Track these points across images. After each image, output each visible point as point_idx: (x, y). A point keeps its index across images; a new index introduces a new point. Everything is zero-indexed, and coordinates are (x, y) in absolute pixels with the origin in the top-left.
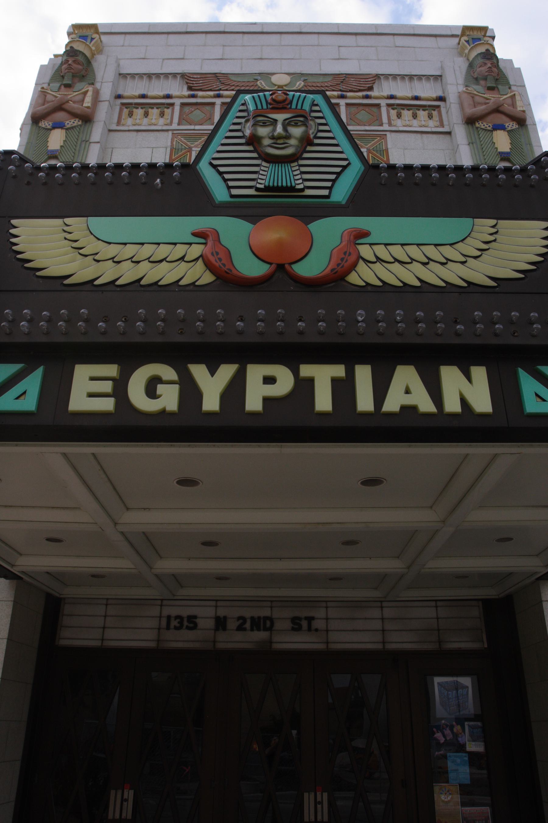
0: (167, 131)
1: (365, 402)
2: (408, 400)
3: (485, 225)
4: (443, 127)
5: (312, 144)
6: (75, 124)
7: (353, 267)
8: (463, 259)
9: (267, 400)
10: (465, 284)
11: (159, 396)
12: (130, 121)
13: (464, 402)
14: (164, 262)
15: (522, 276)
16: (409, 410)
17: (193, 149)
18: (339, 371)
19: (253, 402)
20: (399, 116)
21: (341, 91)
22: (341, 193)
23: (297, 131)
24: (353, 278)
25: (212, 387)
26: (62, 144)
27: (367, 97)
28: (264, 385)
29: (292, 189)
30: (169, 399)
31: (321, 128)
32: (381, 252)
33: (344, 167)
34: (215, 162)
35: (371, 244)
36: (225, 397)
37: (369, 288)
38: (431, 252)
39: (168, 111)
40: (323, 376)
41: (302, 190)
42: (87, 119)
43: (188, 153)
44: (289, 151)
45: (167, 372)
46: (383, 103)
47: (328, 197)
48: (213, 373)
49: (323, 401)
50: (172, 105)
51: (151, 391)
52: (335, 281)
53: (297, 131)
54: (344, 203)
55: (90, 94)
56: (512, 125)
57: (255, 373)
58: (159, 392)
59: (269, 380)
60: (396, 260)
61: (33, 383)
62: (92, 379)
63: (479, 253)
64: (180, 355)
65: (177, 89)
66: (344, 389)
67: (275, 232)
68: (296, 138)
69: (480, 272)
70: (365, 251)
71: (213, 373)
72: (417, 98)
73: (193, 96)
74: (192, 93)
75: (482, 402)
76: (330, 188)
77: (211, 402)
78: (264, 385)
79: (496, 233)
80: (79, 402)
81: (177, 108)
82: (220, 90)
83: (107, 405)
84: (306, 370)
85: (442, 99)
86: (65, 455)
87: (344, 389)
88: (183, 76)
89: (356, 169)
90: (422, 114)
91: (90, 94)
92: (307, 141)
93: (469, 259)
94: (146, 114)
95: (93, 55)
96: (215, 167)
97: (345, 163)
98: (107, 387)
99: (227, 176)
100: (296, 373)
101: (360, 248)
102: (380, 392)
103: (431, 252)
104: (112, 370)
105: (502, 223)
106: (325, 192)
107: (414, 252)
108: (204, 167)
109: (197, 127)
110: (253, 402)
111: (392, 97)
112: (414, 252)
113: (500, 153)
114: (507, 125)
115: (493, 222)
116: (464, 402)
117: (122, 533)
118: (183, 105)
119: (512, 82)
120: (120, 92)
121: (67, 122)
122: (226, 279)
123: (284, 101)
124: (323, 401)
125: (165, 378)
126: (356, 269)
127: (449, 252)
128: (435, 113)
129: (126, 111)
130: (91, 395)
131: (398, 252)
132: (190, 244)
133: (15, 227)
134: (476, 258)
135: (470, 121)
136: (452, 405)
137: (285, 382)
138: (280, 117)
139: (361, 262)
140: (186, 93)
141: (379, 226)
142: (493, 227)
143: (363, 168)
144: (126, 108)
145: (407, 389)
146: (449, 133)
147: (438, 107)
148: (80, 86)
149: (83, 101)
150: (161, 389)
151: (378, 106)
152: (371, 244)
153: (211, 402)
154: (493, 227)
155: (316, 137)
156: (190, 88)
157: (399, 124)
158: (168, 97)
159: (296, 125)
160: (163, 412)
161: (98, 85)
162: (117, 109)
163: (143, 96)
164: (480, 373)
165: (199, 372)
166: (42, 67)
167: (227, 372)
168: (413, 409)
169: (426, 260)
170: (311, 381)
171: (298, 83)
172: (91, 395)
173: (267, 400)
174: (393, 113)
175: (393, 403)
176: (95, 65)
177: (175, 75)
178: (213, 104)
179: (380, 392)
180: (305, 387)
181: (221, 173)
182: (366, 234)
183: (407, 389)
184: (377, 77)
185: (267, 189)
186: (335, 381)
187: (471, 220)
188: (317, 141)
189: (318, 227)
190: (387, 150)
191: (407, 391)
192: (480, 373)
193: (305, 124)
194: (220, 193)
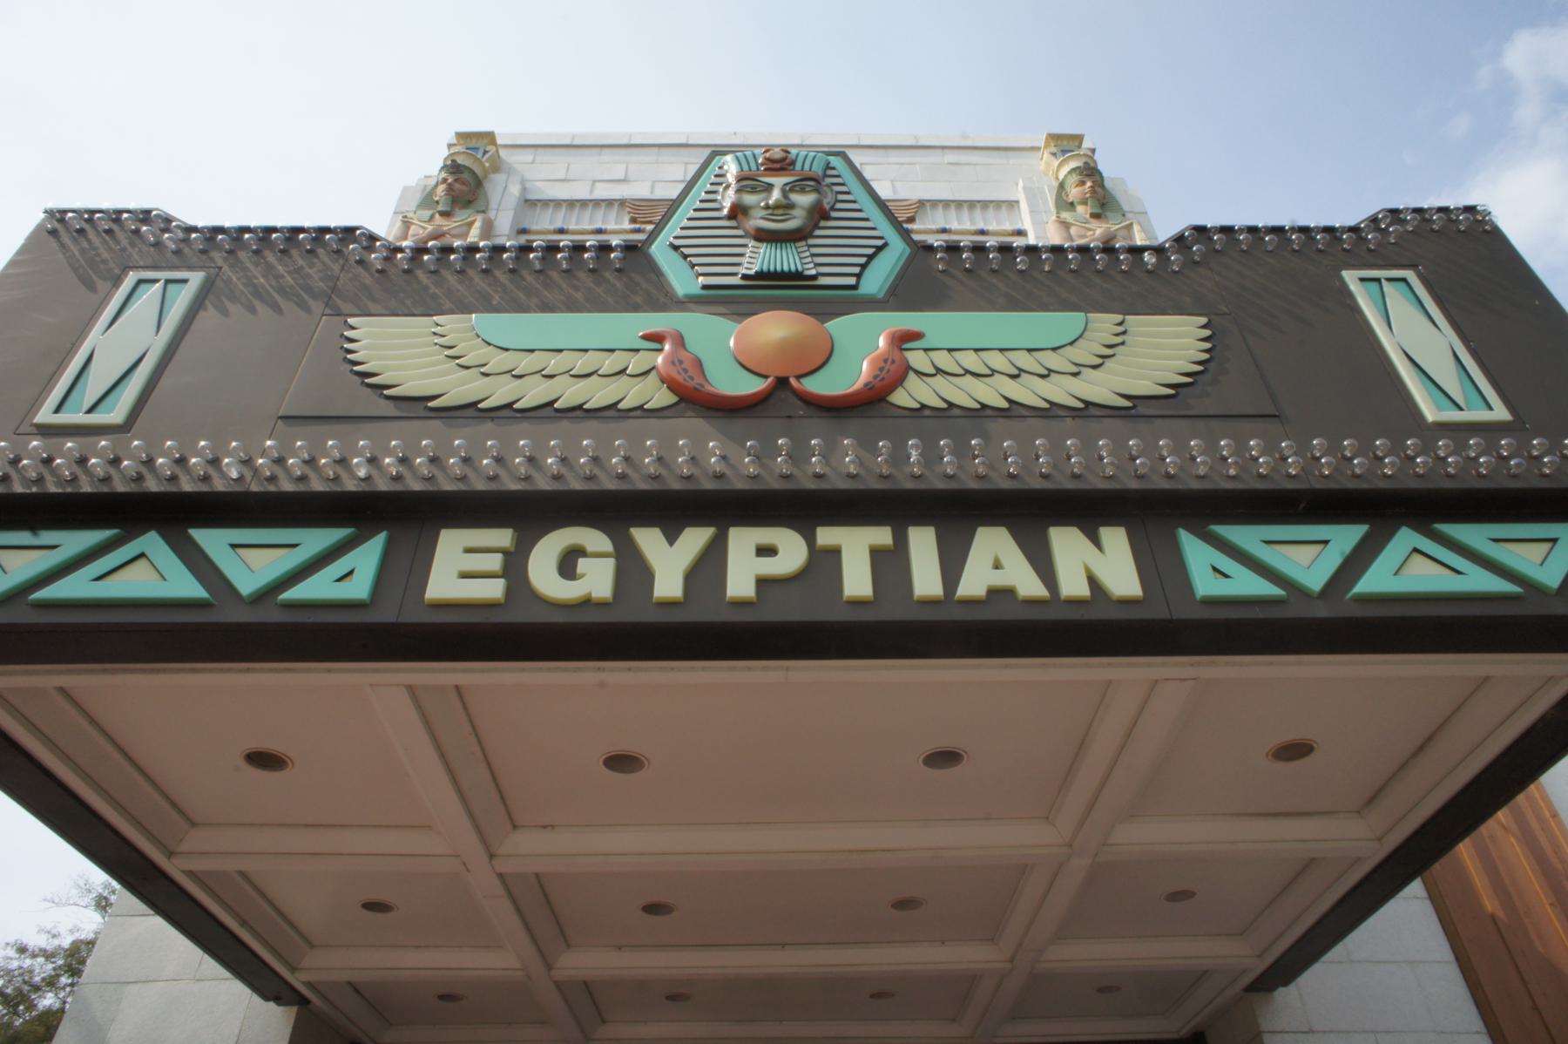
1: (926, 579)
2: (1000, 579)
3: (1104, 324)
5: (827, 217)
7: (898, 381)
8: (1075, 369)
9: (762, 583)
10: (1081, 405)
11: (582, 576)
13: (1093, 581)
14: (594, 377)
15: (1172, 392)
18: (882, 536)
22: (876, 280)
23: (804, 200)
24: (900, 398)
28: (755, 561)
29: (798, 275)
31: (841, 197)
32: (943, 360)
33: (879, 249)
34: (677, 242)
35: (926, 350)
36: (691, 576)
37: (927, 412)
38: (1024, 360)
40: (855, 547)
41: (814, 277)
44: (792, 224)
45: (595, 539)
47: (854, 287)
48: (671, 540)
49: (857, 581)
51: (568, 565)
52: (869, 404)
53: (804, 200)
54: (881, 295)
55: (477, 224)
57: (742, 541)
58: (579, 570)
59: (766, 551)
60: (967, 372)
61: (366, 559)
62: (469, 550)
63: (1099, 361)
64: (616, 510)
66: (890, 564)
67: (774, 328)
68: (802, 208)
69: (1101, 388)
70: (917, 359)
71: (671, 540)
73: (638, 231)
76: (859, 276)
77: (668, 583)
78: (755, 561)
79: (1124, 333)
83: (494, 590)
84: (827, 536)
86: (411, 689)
87: (890, 564)
88: (622, 203)
89: (898, 248)
91: (477, 224)
92: (819, 214)
93: (1084, 370)
95: (486, 173)
96: (676, 248)
97: (879, 243)
98: (494, 562)
99: (695, 260)
100: (810, 540)
101: (908, 355)
102: (952, 568)
103: (1024, 360)
104: (502, 537)
105: (1131, 319)
106: (852, 281)
107: (997, 361)
108: (659, 251)
110: (740, 581)
112: (997, 361)
115: (1119, 318)
116: (1093, 581)
117: (501, 876)
119: (1126, 208)
120: (527, 226)
122: (694, 399)
123: (784, 159)
124: (857, 581)
125: (590, 548)
126: (906, 384)
127: (1052, 360)
130: (465, 575)
131: (970, 361)
132: (637, 350)
133: (353, 328)
134: (1095, 367)
136: (1073, 585)
138: (779, 181)
139: (911, 375)
140: (627, 226)
141: (936, 325)
142: (1120, 324)
143: (908, 251)
148: (461, 216)
149: (466, 235)
150: (583, 564)
152: (926, 350)
153: (668, 583)
154: (1120, 324)
155: (833, 209)
156: (633, 220)
159: (803, 191)
160: (587, 603)
161: (492, 214)
164: (1116, 539)
165: (648, 539)
166: (406, 189)
167: (695, 539)
168: (1006, 593)
169: (1016, 372)
170: (835, 553)
172: (465, 575)
173: (762, 583)
175: (973, 584)
176: (487, 186)
179: (952, 568)
180: (825, 563)
181: (685, 257)
182: (917, 336)
183: (995, 564)
184: (921, 203)
185: (760, 275)
186: (876, 554)
187: (1081, 315)
188: (834, 214)
189: (841, 327)
191: (997, 566)
193: (817, 190)
194: (683, 281)
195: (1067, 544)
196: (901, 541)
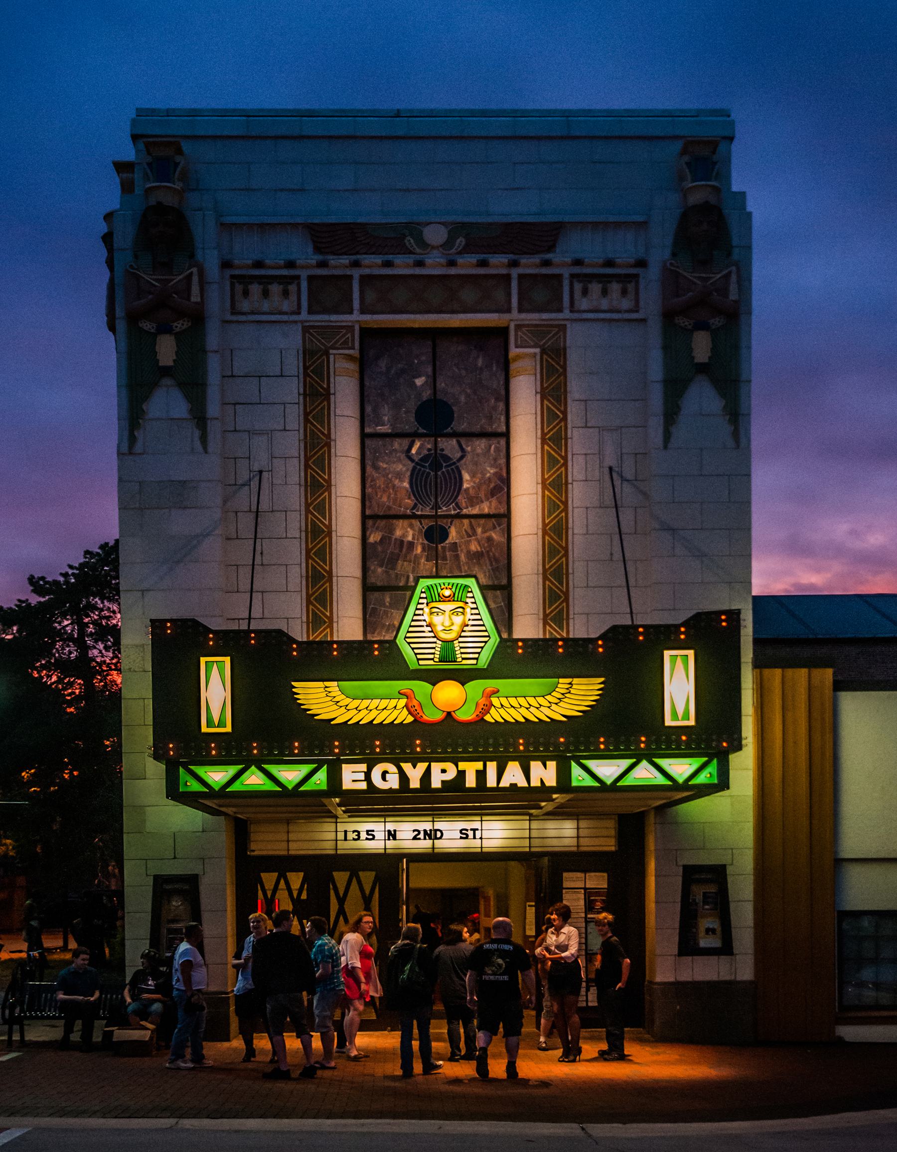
0: (296, 322)
1: (491, 782)
4: (637, 311)
6: (185, 327)
9: (443, 782)
12: (245, 306)
16: (514, 786)
17: (331, 351)
18: (479, 765)
19: (436, 783)
20: (585, 292)
21: (513, 253)
25: (415, 774)
26: (175, 358)
27: (547, 263)
28: (441, 774)
30: (393, 782)
39: (293, 288)
40: (471, 768)
42: (198, 318)
43: (325, 357)
45: (391, 768)
46: (566, 272)
49: (471, 781)
50: (298, 277)
51: (384, 778)
56: (717, 322)
57: (436, 767)
59: (444, 771)
65: (303, 253)
66: (481, 775)
72: (610, 263)
73: (323, 264)
74: (320, 257)
75: (551, 782)
77: (415, 784)
78: (441, 774)
80: (348, 783)
81: (304, 285)
82: (357, 253)
83: (363, 786)
84: (462, 765)
85: (642, 263)
87: (481, 775)
90: (615, 287)
94: (266, 294)
98: (362, 776)
100: (457, 766)
104: (363, 767)
109: (334, 317)
110: (436, 783)
111: (578, 262)
113: (697, 364)
114: (712, 321)
118: (311, 278)
121: (175, 324)
124: (471, 781)
128: (631, 287)
129: (239, 288)
135: (668, 316)
136: (535, 783)
137: (451, 774)
140: (314, 259)
144: (240, 283)
145: (514, 775)
146: (644, 320)
147: (636, 276)
151: (559, 277)
153: (415, 784)
156: (318, 250)
157: (584, 304)
158: (291, 264)
160: (391, 790)
162: (228, 283)
163: (259, 264)
164: (552, 765)
165: (407, 767)
167: (422, 767)
171: (458, 241)
174: (578, 287)
177: (295, 226)
178: (350, 277)
180: (461, 774)
190: (565, 349)
192: (552, 765)
195: (536, 767)
196: (485, 766)
